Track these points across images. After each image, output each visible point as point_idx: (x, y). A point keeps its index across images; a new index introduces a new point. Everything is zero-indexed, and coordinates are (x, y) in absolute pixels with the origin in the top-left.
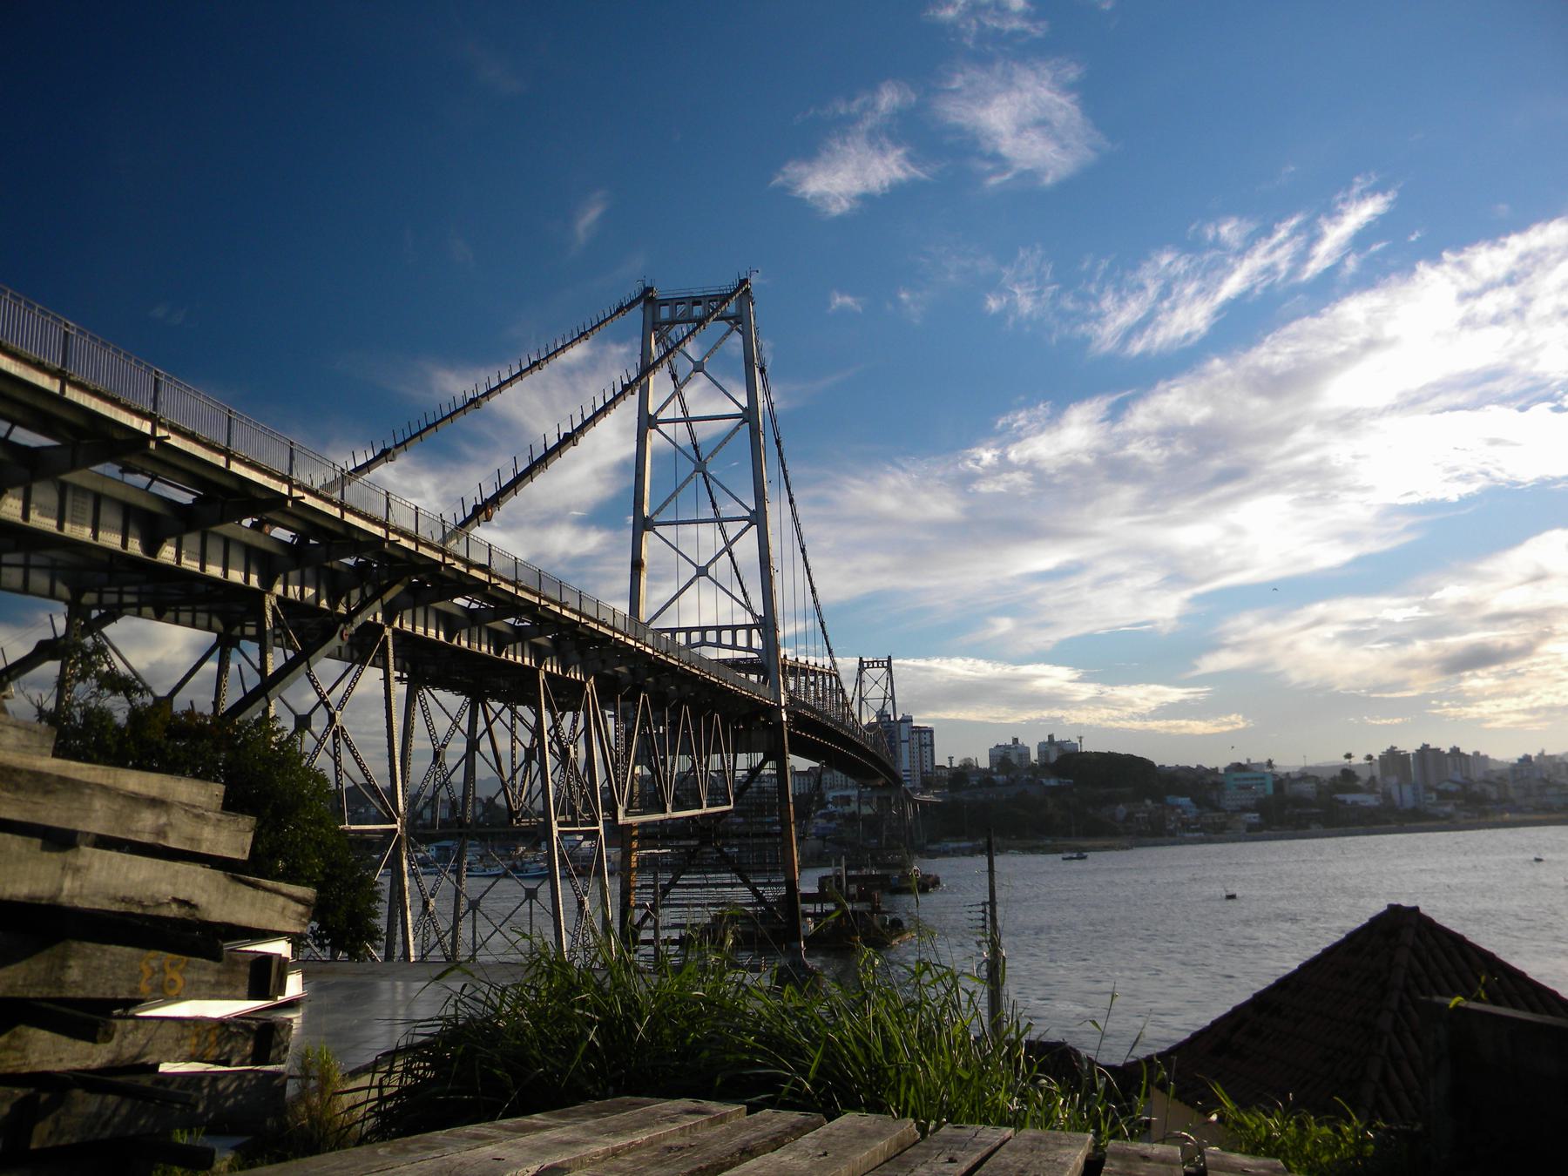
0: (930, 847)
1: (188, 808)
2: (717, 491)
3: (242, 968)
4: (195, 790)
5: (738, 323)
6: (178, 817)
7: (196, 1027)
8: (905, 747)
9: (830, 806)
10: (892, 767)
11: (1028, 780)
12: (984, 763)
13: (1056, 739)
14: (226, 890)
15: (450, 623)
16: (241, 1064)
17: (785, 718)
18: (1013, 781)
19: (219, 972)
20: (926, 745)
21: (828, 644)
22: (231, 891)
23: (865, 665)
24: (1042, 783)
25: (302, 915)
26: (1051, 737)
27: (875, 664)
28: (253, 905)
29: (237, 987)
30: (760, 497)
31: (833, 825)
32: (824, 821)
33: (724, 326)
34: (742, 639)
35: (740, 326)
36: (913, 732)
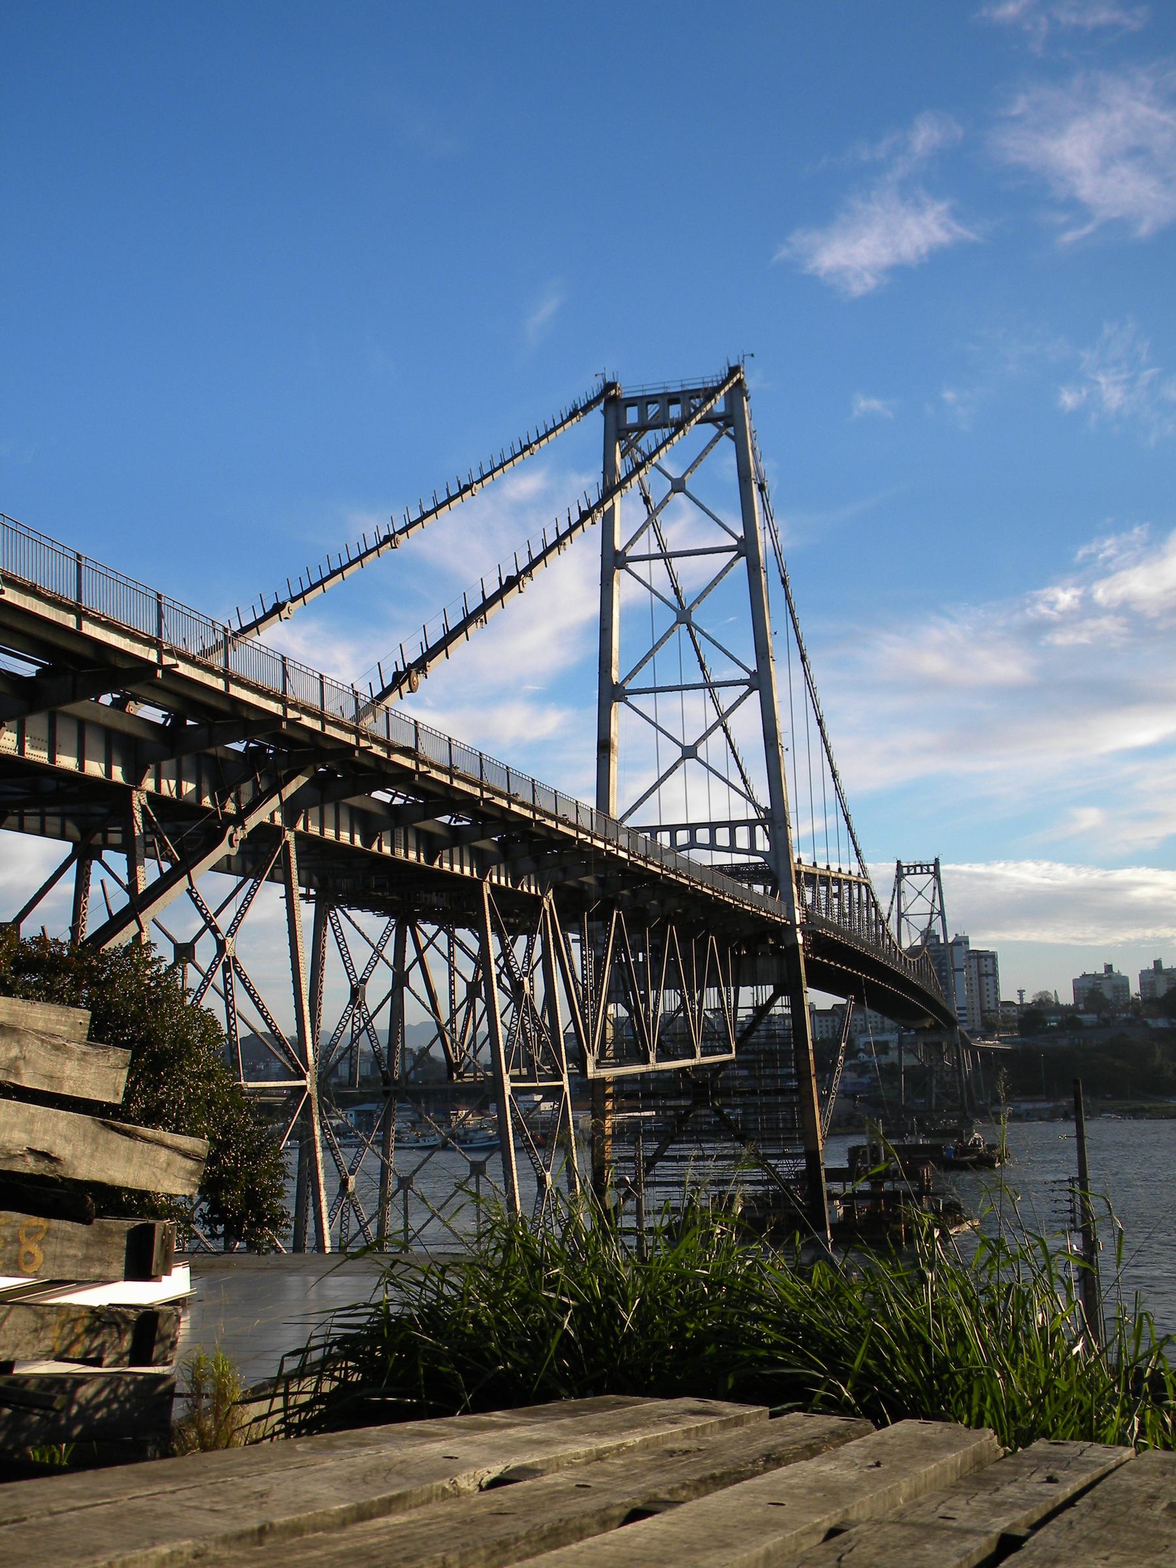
1: (46, 1037)
2: (706, 647)
3: (117, 1239)
4: (53, 1017)
5: (727, 425)
6: (33, 1048)
7: (59, 1315)
10: (943, 1004)
11: (1125, 1020)
12: (1067, 998)
13: (1165, 966)
14: (95, 1140)
15: (368, 823)
16: (115, 1364)
19: (88, 1244)
20: (987, 975)
21: (854, 843)
22: (101, 1141)
23: (905, 870)
24: (1145, 1023)
25: (192, 1173)
28: (129, 1160)
29: (110, 1263)
30: (762, 653)
31: (865, 1080)
32: (854, 1075)
33: (710, 430)
34: (742, 841)
35: (731, 430)
36: (970, 958)
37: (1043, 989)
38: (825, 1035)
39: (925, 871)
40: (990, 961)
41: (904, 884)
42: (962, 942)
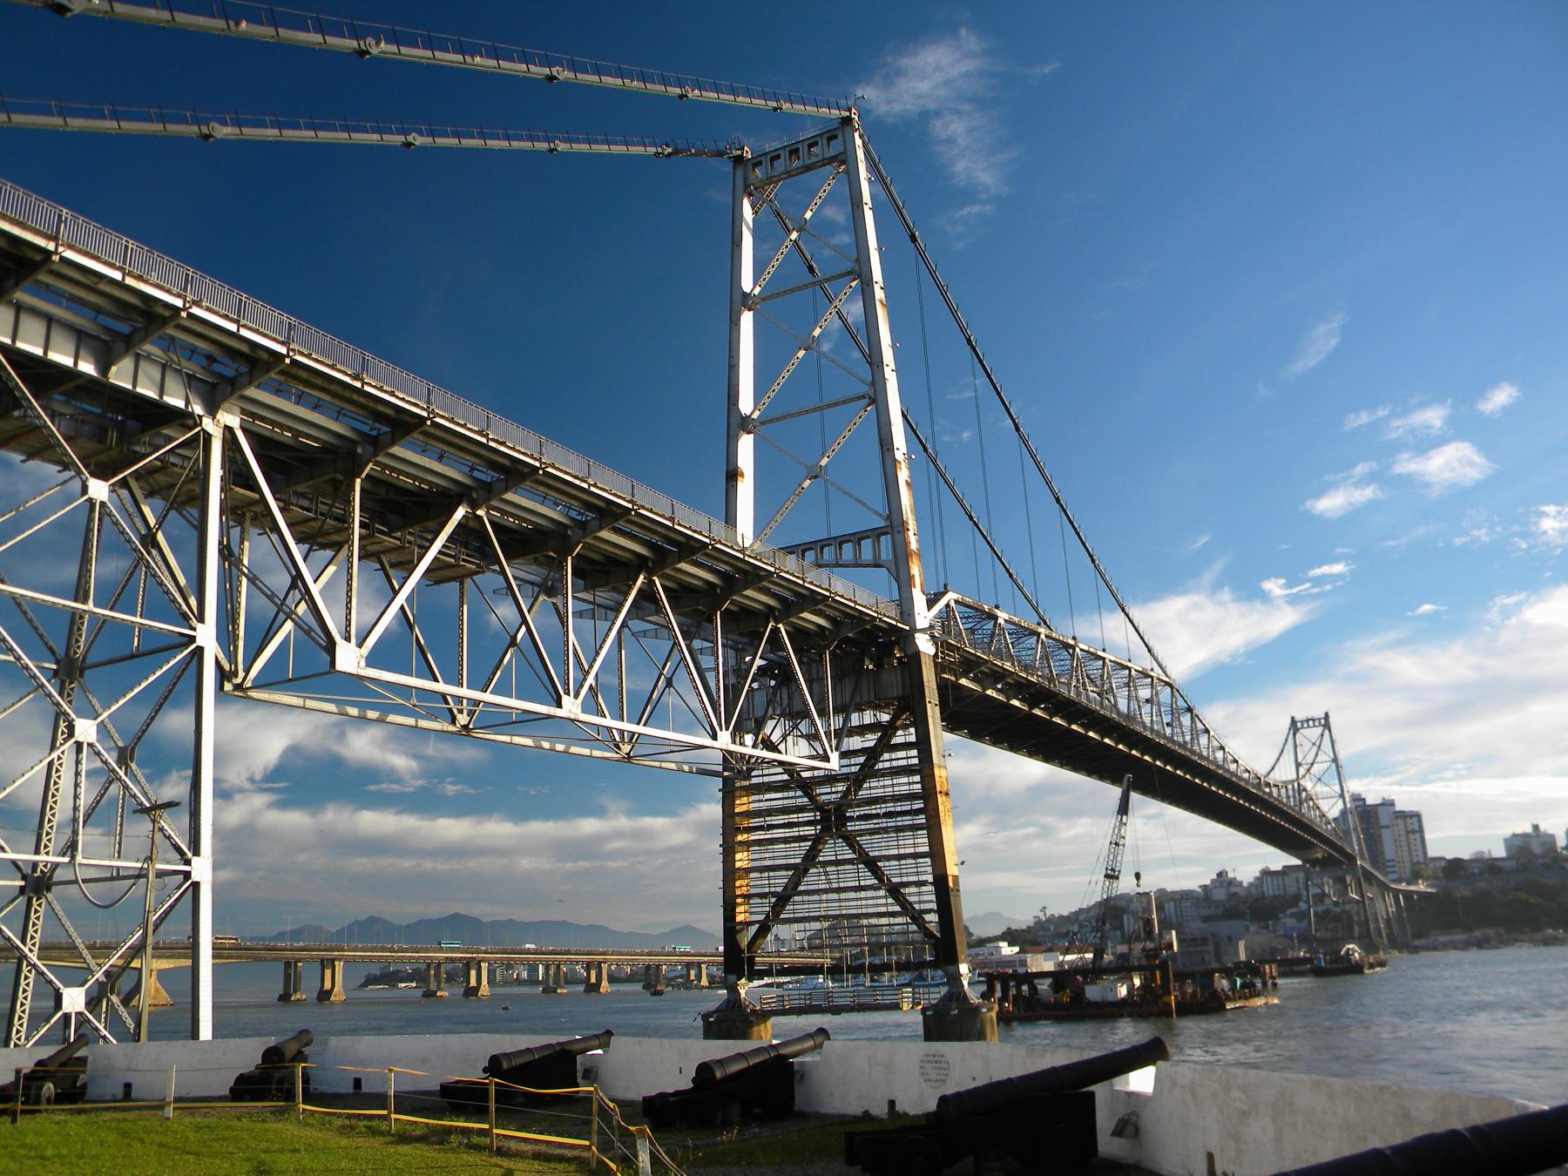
0: (1417, 942)
5: (843, 162)
8: (1386, 834)
12: (1500, 852)
17: (925, 645)
20: (1414, 832)
23: (1299, 725)
27: (1311, 723)
36: (1397, 818)
38: (1277, 893)
39: (1317, 724)
40: (1415, 819)
41: (1298, 736)
42: (1388, 804)
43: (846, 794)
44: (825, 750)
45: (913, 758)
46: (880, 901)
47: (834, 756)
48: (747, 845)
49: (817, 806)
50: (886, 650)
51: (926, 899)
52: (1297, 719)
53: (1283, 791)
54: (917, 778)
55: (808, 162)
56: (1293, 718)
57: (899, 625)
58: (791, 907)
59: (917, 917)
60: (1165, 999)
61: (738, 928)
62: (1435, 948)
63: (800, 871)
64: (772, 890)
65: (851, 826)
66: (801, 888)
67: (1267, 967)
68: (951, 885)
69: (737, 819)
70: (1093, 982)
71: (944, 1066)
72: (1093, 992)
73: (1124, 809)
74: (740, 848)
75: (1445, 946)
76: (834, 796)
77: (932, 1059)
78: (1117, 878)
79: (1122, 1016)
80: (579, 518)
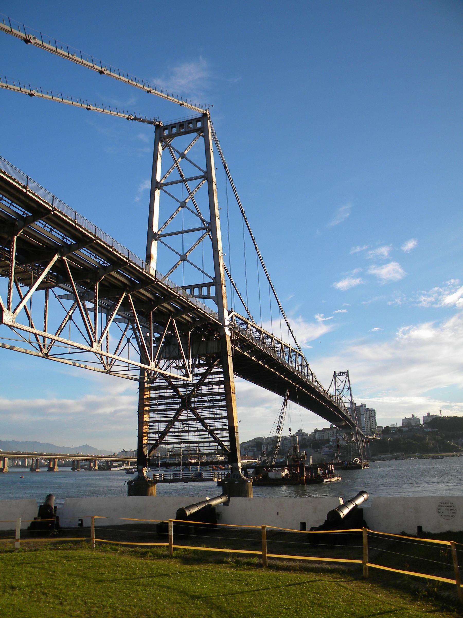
0: (373, 457)
5: (202, 132)
9: (330, 443)
11: (417, 429)
12: (400, 424)
13: (431, 414)
18: (410, 429)
20: (372, 417)
23: (337, 374)
24: (424, 430)
26: (429, 414)
27: (341, 374)
36: (366, 411)
37: (393, 424)
40: (373, 412)
41: (336, 378)
43: (192, 392)
44: (188, 373)
45: (221, 378)
46: (206, 436)
47: (191, 376)
48: (149, 411)
49: (179, 396)
50: (211, 333)
51: (224, 436)
52: (336, 372)
53: (334, 398)
54: (223, 386)
55: (187, 130)
56: (335, 372)
57: (219, 323)
58: (166, 438)
59: (220, 443)
60: (302, 478)
61: (144, 446)
62: (380, 460)
63: (171, 423)
64: (160, 430)
65: (193, 405)
66: (171, 430)
67: (331, 466)
68: (235, 430)
69: (145, 401)
70: (271, 471)
71: (454, 508)
72: (271, 475)
73: (285, 403)
74: (146, 413)
75: (383, 459)
76: (188, 392)
77: (445, 505)
78: (282, 430)
79: (284, 484)
80: (104, 265)
